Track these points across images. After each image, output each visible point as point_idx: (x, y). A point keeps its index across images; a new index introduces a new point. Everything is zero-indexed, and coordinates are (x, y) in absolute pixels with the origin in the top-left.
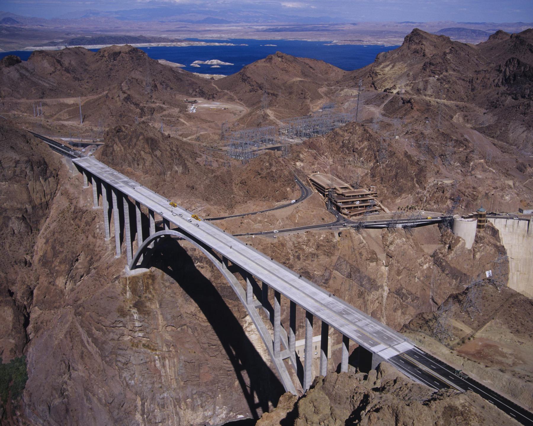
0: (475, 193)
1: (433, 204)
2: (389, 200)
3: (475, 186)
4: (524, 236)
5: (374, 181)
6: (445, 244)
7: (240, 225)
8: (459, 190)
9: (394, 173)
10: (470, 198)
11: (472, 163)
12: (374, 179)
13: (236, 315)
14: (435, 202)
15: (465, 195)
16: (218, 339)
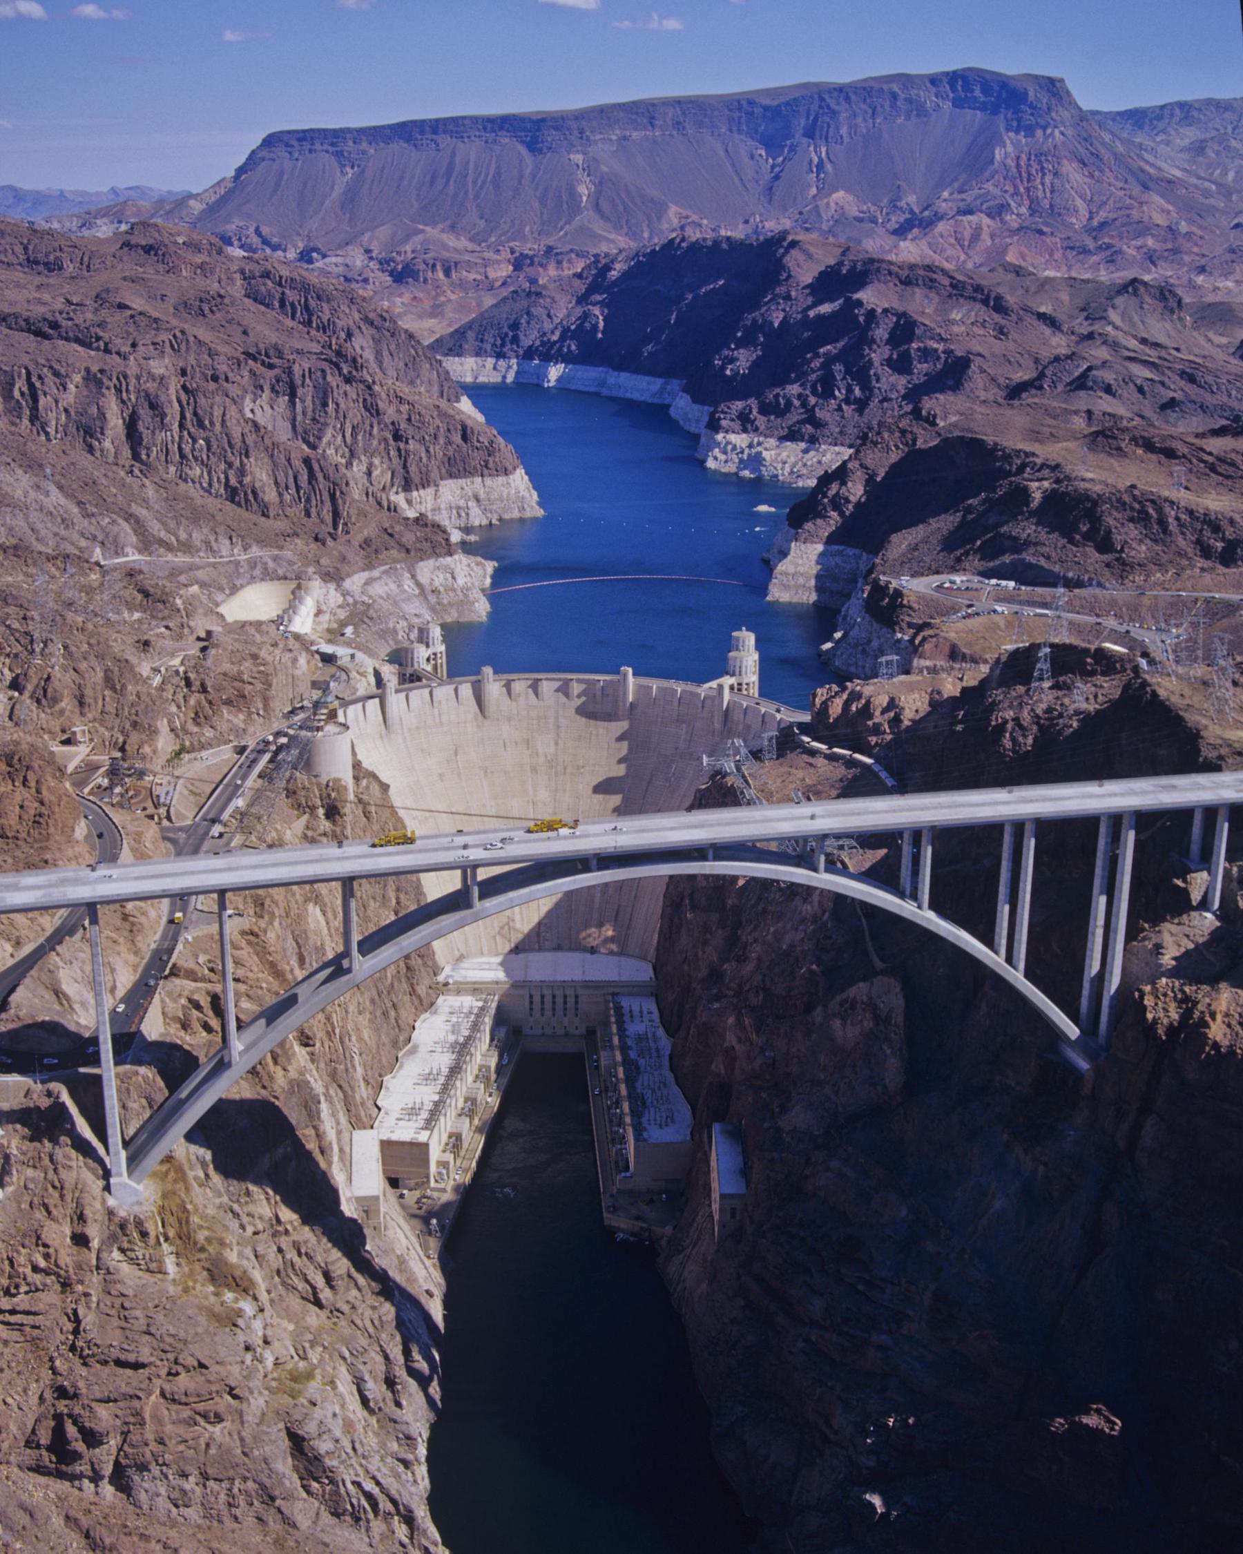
0: (262, 668)
1: (196, 729)
2: (147, 749)
3: (254, 650)
4: (381, 737)
5: (62, 712)
6: (313, 809)
7: (127, 926)
8: (225, 674)
9: (100, 675)
10: (259, 686)
11: (179, 602)
12: (57, 708)
13: (323, 1165)
14: (198, 724)
15: (243, 682)
16: (339, 1254)
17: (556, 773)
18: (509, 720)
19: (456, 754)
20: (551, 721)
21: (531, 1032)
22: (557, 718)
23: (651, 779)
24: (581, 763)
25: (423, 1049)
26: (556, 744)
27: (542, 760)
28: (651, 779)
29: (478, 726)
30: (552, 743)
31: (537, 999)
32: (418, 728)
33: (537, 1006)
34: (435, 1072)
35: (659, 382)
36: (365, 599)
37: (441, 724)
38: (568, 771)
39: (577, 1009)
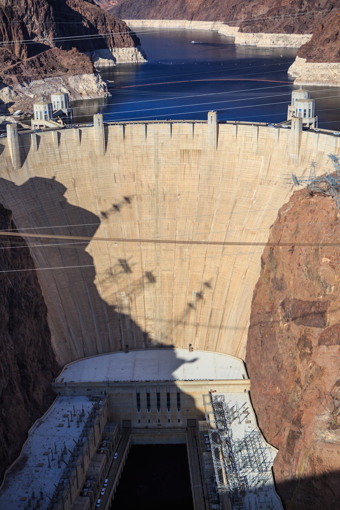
17: (157, 201)
18: (118, 158)
19: (75, 186)
20: (153, 157)
21: (139, 425)
22: (157, 156)
23: (235, 202)
24: (177, 192)
25: (31, 462)
26: (157, 176)
27: (145, 190)
28: (235, 202)
29: (93, 163)
30: (154, 175)
31: (143, 397)
32: (41, 164)
33: (144, 402)
34: (38, 495)
35: (212, 23)
36: (32, 96)
37: (62, 162)
38: (167, 197)
39: (179, 405)
